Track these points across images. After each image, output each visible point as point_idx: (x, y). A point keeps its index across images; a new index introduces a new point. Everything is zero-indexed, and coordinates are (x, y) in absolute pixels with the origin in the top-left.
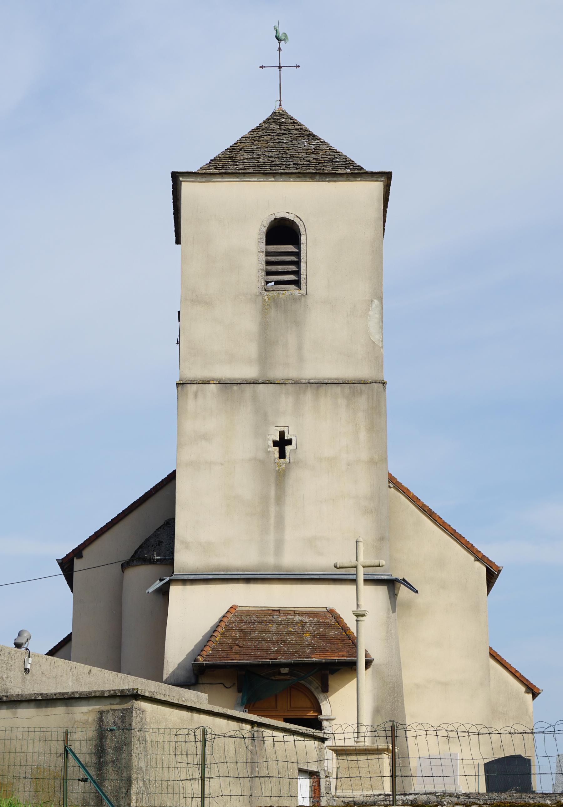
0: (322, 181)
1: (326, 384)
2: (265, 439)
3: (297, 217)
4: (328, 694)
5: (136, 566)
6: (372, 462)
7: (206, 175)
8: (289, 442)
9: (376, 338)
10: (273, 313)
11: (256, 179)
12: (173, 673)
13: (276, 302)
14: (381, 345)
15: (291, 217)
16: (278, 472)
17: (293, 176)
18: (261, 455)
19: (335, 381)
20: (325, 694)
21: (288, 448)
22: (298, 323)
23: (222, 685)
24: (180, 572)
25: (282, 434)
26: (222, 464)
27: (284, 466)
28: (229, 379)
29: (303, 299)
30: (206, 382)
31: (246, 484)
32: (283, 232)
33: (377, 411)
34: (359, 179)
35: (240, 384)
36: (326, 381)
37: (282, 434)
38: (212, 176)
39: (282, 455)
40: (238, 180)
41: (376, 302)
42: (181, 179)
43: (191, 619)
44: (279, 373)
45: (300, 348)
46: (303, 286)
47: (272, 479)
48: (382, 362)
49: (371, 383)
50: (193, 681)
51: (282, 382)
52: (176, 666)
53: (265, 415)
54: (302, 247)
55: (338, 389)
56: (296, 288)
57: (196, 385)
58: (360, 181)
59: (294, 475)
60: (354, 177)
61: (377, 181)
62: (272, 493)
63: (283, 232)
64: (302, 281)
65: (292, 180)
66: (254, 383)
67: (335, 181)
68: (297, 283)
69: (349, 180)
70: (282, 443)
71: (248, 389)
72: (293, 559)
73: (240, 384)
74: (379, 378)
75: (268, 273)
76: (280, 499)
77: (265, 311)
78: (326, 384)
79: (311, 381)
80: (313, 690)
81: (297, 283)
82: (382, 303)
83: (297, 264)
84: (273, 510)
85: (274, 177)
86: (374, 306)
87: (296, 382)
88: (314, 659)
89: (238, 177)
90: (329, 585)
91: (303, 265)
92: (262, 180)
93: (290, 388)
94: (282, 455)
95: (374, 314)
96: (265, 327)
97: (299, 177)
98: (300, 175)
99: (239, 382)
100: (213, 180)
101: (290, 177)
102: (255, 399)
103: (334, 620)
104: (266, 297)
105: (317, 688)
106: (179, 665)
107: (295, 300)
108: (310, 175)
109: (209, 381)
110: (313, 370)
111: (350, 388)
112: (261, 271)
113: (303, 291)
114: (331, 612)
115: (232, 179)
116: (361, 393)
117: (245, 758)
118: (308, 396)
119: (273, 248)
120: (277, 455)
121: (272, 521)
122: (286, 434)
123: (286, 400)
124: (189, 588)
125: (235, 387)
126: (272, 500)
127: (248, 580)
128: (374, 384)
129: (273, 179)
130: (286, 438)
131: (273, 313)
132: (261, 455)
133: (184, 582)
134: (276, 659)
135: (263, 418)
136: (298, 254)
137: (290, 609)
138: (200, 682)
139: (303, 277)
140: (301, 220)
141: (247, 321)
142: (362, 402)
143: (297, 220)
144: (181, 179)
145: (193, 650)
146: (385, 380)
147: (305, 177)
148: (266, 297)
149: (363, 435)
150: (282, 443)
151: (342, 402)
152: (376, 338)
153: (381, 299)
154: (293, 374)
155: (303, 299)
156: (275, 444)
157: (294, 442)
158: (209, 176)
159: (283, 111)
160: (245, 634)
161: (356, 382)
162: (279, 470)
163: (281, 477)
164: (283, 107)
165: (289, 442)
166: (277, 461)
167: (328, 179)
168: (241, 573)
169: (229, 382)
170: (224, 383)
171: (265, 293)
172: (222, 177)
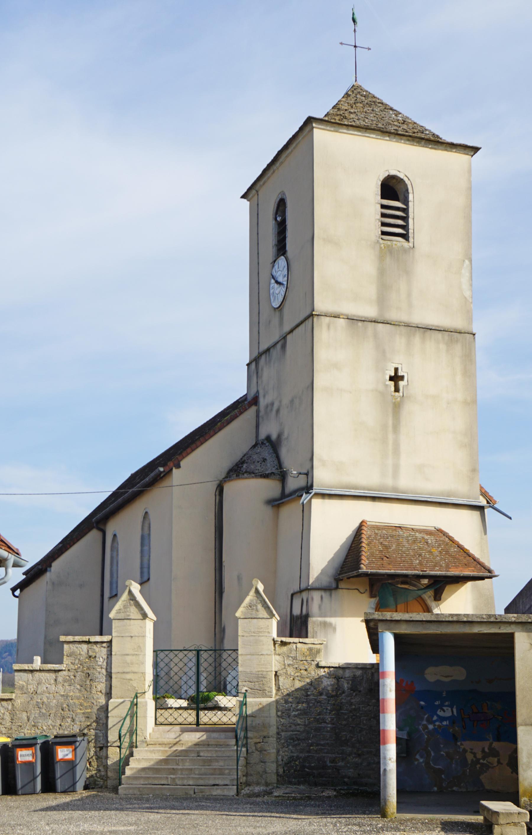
0: (426, 147)
1: (431, 329)
2: (384, 374)
3: (406, 176)
4: (439, 602)
5: (246, 478)
6: (466, 403)
7: (335, 125)
8: (402, 378)
9: (467, 294)
10: (388, 259)
11: (374, 136)
12: (318, 578)
13: (390, 250)
14: (471, 301)
15: (401, 176)
16: (394, 404)
17: (405, 138)
18: (381, 388)
19: (437, 329)
20: (436, 602)
21: (401, 384)
22: (407, 272)
23: (357, 591)
24: (318, 487)
25: (396, 370)
26: (350, 392)
27: (399, 399)
28: (354, 316)
29: (411, 251)
30: (337, 316)
31: (370, 413)
32: (392, 189)
33: (469, 357)
34: (454, 150)
35: (364, 321)
36: (431, 327)
37: (396, 370)
38: (340, 126)
39: (397, 390)
40: (360, 134)
41: (467, 262)
42: (314, 125)
43: (329, 529)
44: (393, 315)
45: (409, 295)
46: (411, 239)
47: (390, 410)
48: (472, 316)
49: (465, 333)
50: (334, 585)
51: (397, 323)
52: (320, 571)
53: (384, 352)
54: (411, 204)
55: (439, 335)
56: (404, 240)
57: (328, 318)
58: (455, 152)
59: (408, 408)
60: (451, 148)
61: (467, 154)
62: (390, 422)
63: (392, 189)
64: (410, 235)
65: (403, 141)
66: (375, 322)
67: (435, 149)
68: (405, 237)
69: (446, 150)
70: (396, 378)
71: (371, 325)
72: (408, 482)
73: (364, 321)
74: (470, 330)
75: (383, 224)
76: (396, 428)
77: (381, 258)
78: (431, 329)
79: (419, 326)
80: (427, 598)
81: (405, 237)
82: (471, 264)
83: (405, 219)
84: (391, 436)
85: (389, 136)
86: (465, 266)
87: (407, 325)
88: (453, 573)
89: (360, 131)
90: (445, 508)
91: (411, 221)
92: (379, 137)
93: (403, 329)
94: (397, 390)
95: (465, 273)
96: (382, 272)
97: (408, 140)
98: (410, 138)
99: (363, 319)
100: (341, 130)
101: (401, 139)
102: (375, 336)
103: (447, 539)
104: (382, 245)
105: (430, 597)
106: (322, 570)
107: (405, 251)
108: (418, 140)
109: (339, 315)
110: (420, 317)
111: (449, 335)
112: (378, 221)
113: (411, 244)
114: (440, 531)
115: (356, 133)
116: (457, 341)
117: (213, 645)
118: (417, 339)
119: (386, 202)
120: (393, 389)
121: (390, 447)
122: (400, 371)
123: (399, 340)
124: (328, 502)
125: (360, 324)
126: (390, 429)
127: (374, 499)
128: (467, 334)
129: (388, 138)
130: (400, 374)
131: (388, 259)
132: (381, 388)
133: (323, 496)
134: (426, 571)
135: (382, 355)
136: (405, 210)
137: (409, 526)
138: (340, 587)
139: (411, 231)
140: (409, 179)
141: (368, 265)
142: (458, 349)
143: (406, 179)
144: (314, 125)
145: (333, 558)
146: (474, 332)
147: (413, 141)
148: (382, 245)
149: (459, 378)
150: (396, 378)
151: (443, 347)
152: (467, 294)
153: (471, 261)
154: (404, 317)
155: (411, 251)
156: (391, 379)
157: (406, 379)
158: (337, 126)
159: (359, 87)
160: (387, 547)
161: (453, 331)
162: (395, 403)
163: (397, 407)
164: (359, 83)
165: (402, 378)
166: (393, 394)
167: (430, 146)
168: (366, 492)
169: (355, 318)
170: (351, 319)
171: (382, 241)
172: (348, 129)
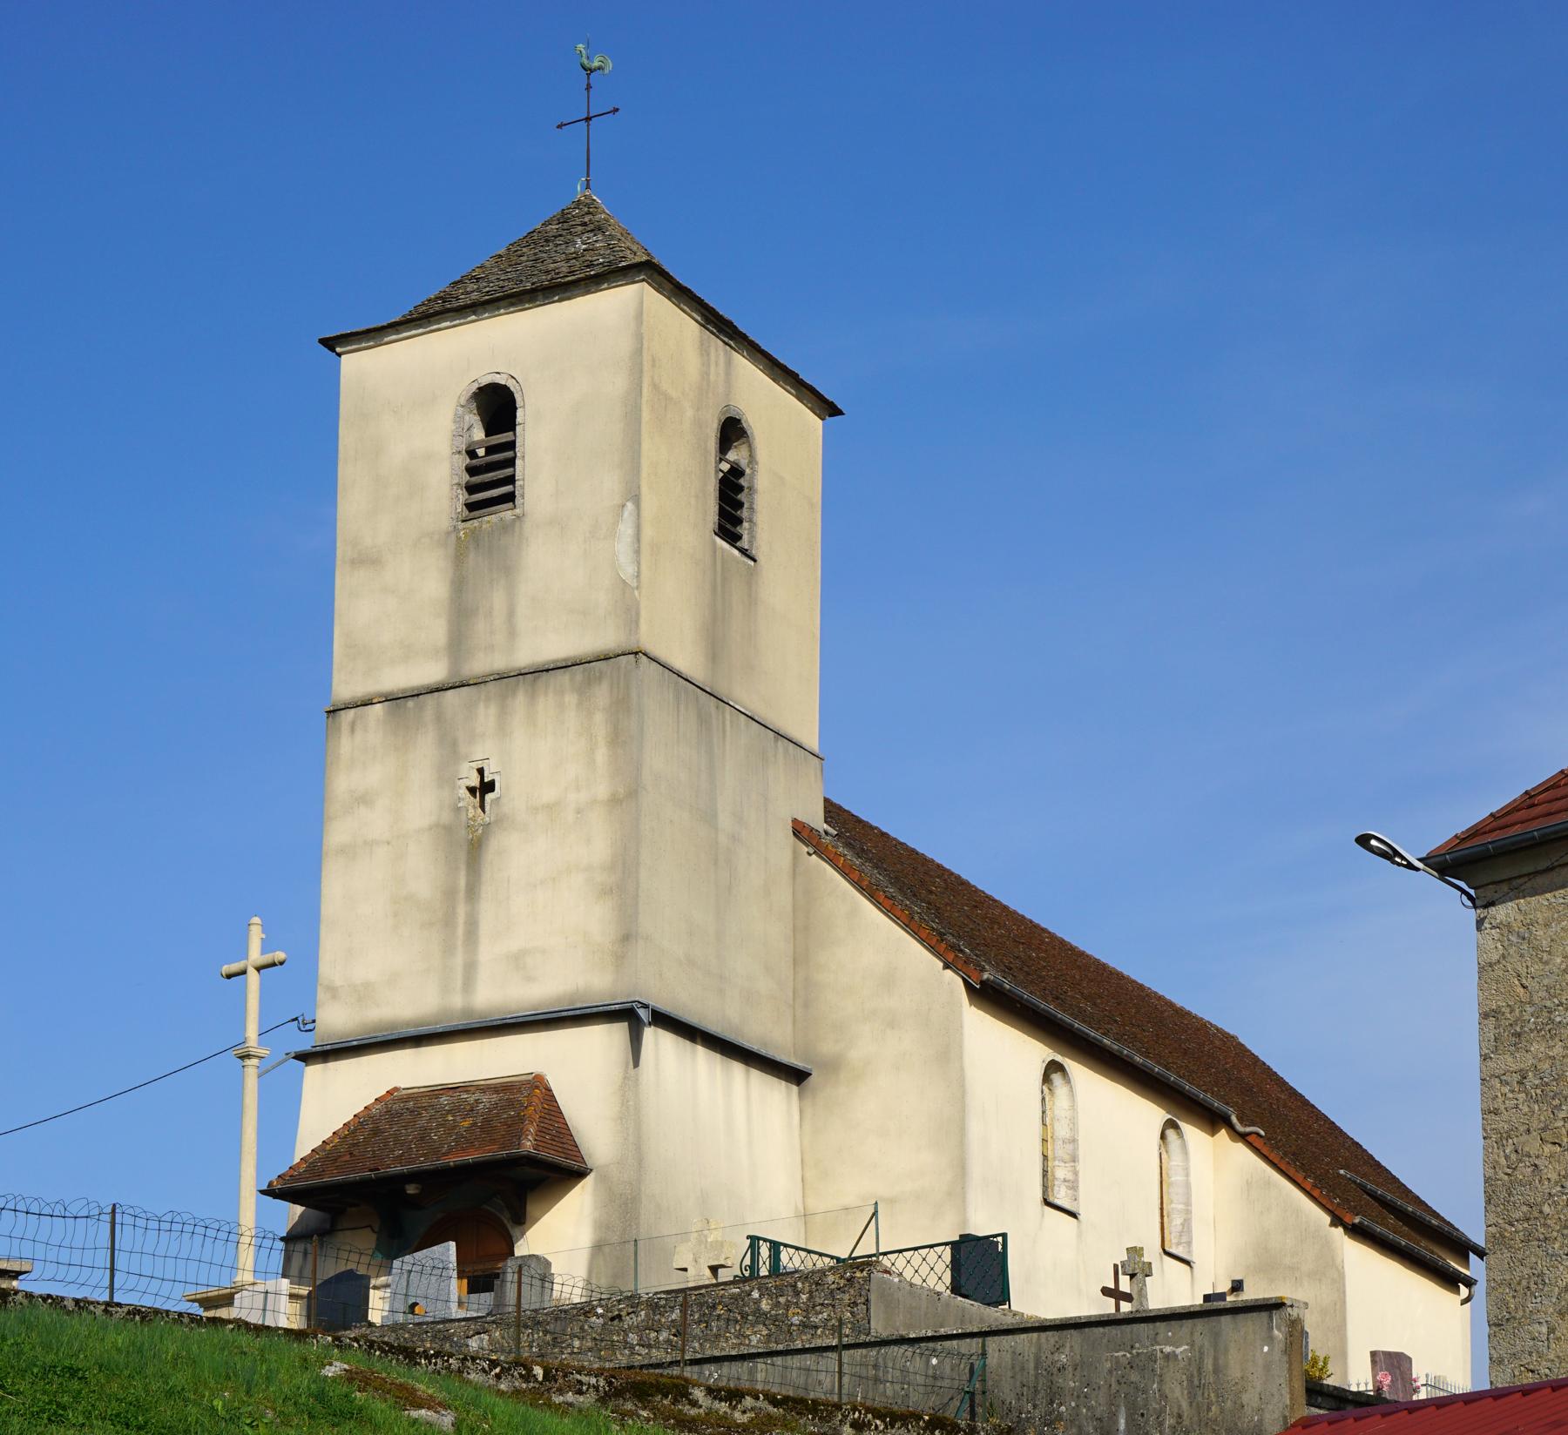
2: (454, 788)
6: (615, 801)
9: (628, 571)
13: (474, 535)
15: (501, 380)
17: (502, 303)
21: (489, 797)
22: (508, 570)
30: (367, 703)
41: (630, 506)
44: (479, 664)
45: (511, 614)
47: (462, 856)
55: (564, 678)
66: (438, 690)
67: (569, 298)
77: (459, 559)
85: (474, 313)
86: (626, 514)
87: (501, 677)
95: (626, 529)
96: (459, 584)
97: (513, 305)
102: (439, 718)
107: (506, 528)
110: (527, 654)
116: (600, 679)
125: (411, 703)
131: (471, 558)
135: (450, 749)
142: (602, 695)
143: (511, 384)
147: (521, 302)
149: (602, 754)
151: (571, 699)
154: (499, 663)
170: (391, 698)
172: (398, 332)
